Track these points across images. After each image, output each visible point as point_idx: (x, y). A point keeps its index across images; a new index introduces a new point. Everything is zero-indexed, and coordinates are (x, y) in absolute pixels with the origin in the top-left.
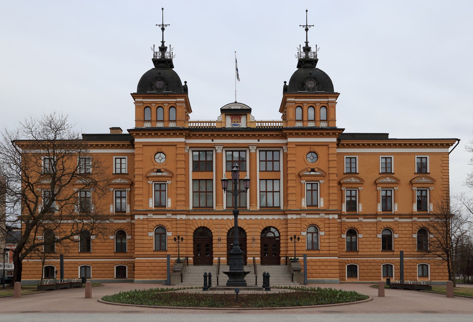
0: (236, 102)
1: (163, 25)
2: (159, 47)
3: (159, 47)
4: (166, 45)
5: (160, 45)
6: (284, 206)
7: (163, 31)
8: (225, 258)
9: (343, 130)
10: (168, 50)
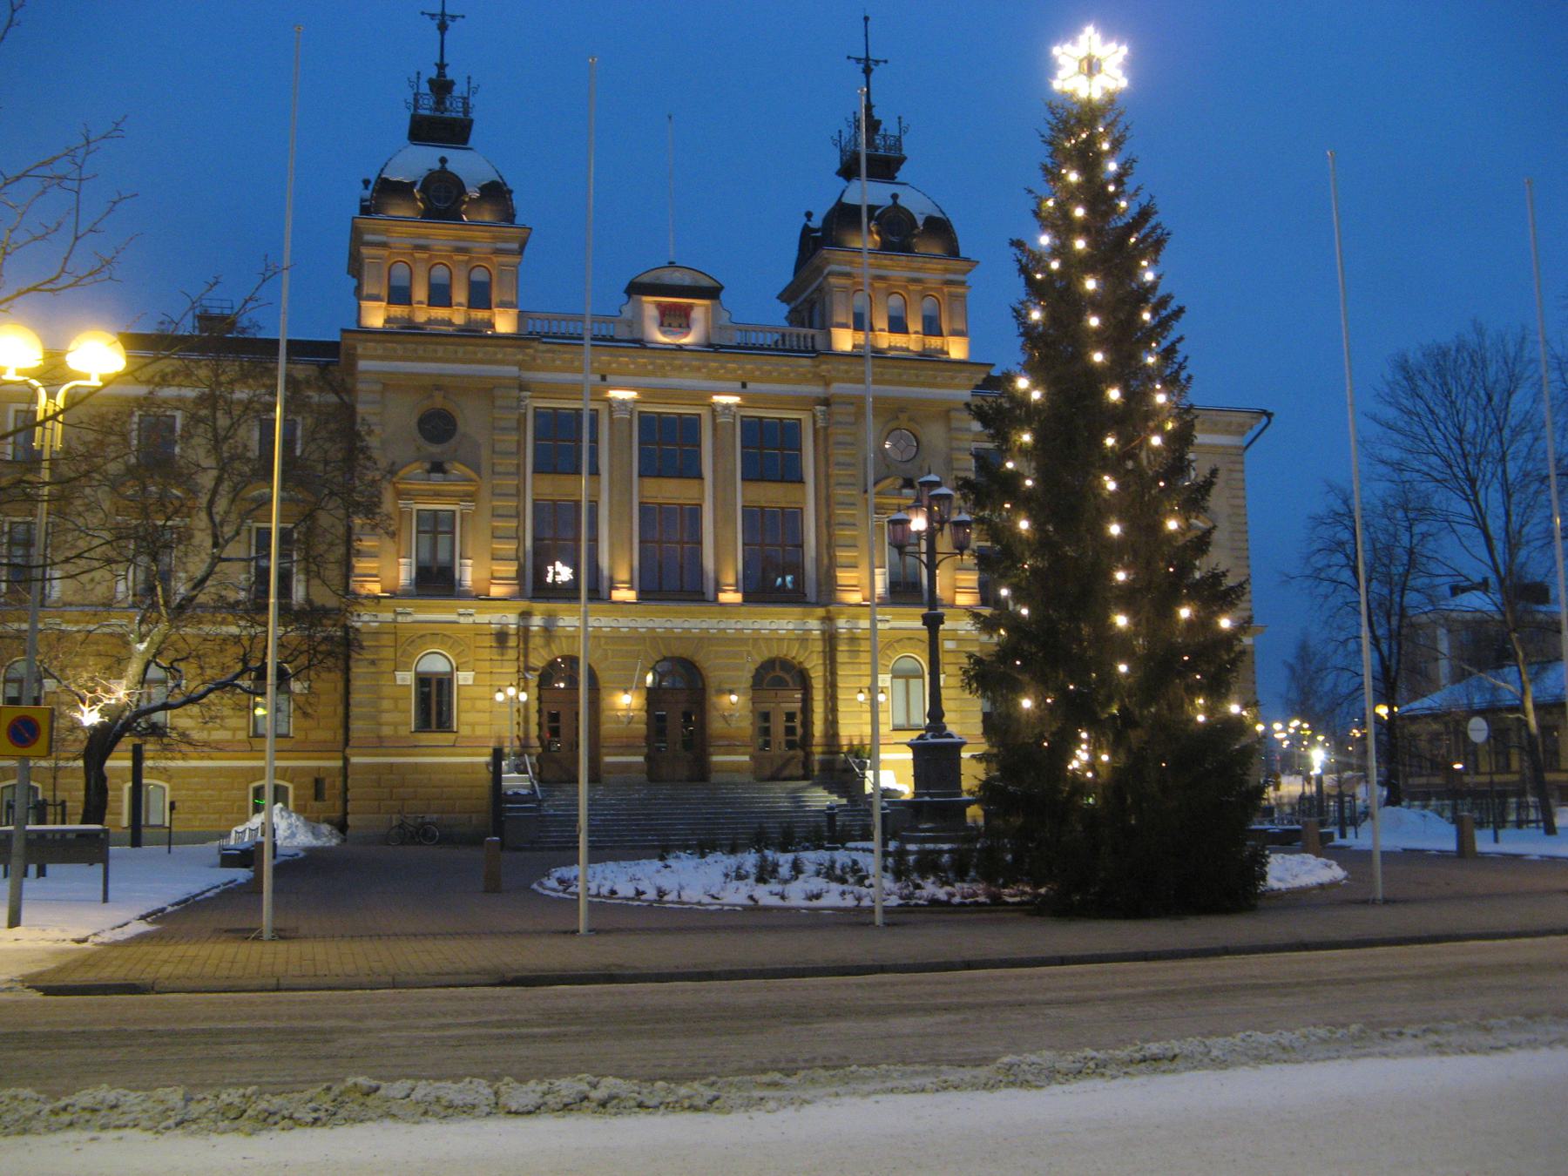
0: (671, 264)
1: (443, 14)
2: (431, 81)
3: (431, 81)
4: (450, 74)
5: (433, 73)
6: (819, 592)
7: (442, 35)
8: (640, 759)
9: (992, 365)
10: (459, 90)
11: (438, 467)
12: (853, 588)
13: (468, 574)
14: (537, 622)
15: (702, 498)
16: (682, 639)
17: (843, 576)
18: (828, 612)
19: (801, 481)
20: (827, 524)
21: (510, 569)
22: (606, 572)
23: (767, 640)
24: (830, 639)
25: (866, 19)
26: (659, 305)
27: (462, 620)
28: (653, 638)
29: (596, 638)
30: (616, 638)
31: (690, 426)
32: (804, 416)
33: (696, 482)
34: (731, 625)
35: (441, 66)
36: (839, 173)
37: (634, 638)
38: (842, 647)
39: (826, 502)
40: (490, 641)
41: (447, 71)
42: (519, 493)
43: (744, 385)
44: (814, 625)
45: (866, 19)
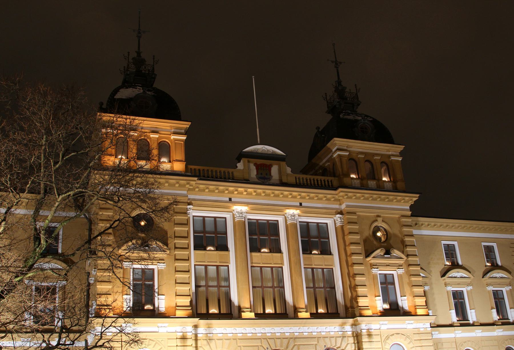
13: (162, 303)
14: (201, 330)
15: (282, 264)
17: (362, 302)
18: (357, 321)
19: (330, 254)
20: (350, 276)
21: (186, 301)
22: (236, 303)
24: (357, 337)
25: (334, 45)
26: (255, 164)
27: (161, 330)
31: (274, 227)
32: (329, 222)
35: (139, 53)
36: (328, 112)
38: (365, 339)
39: (347, 264)
41: (141, 55)
43: (301, 204)
44: (348, 328)
45: (334, 45)
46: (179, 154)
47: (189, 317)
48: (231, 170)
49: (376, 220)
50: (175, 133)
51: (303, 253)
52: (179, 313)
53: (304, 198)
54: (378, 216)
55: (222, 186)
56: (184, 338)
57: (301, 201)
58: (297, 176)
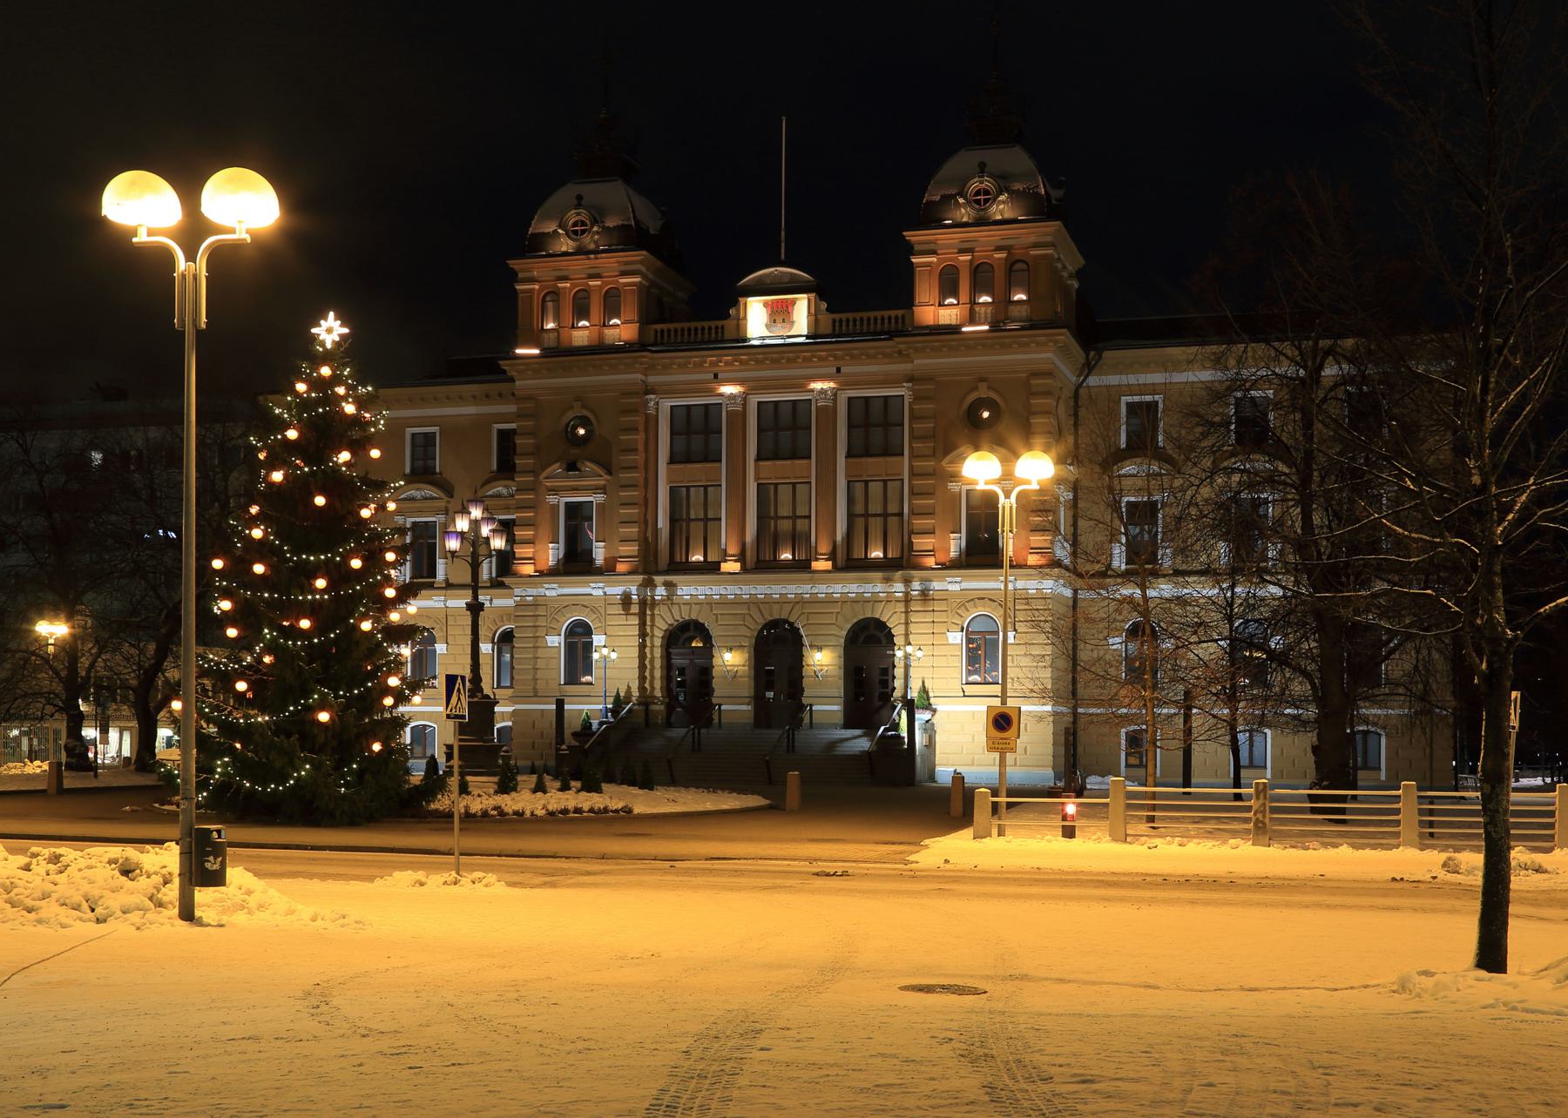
11: (572, 466)
12: (932, 552)
13: (599, 554)
16: (783, 601)
17: (921, 542)
21: (632, 549)
23: (854, 601)
26: (766, 304)
27: (595, 592)
28: (754, 603)
29: (709, 603)
30: (724, 602)
33: (805, 462)
34: (822, 590)
37: (737, 602)
40: (618, 610)
42: (650, 484)
43: (838, 370)
46: (630, 309)
47: (630, 573)
48: (720, 323)
49: (976, 388)
50: (624, 274)
51: (849, 455)
52: (621, 567)
53: (842, 358)
54: (982, 380)
55: (695, 357)
56: (626, 600)
57: (838, 363)
58: (837, 316)
